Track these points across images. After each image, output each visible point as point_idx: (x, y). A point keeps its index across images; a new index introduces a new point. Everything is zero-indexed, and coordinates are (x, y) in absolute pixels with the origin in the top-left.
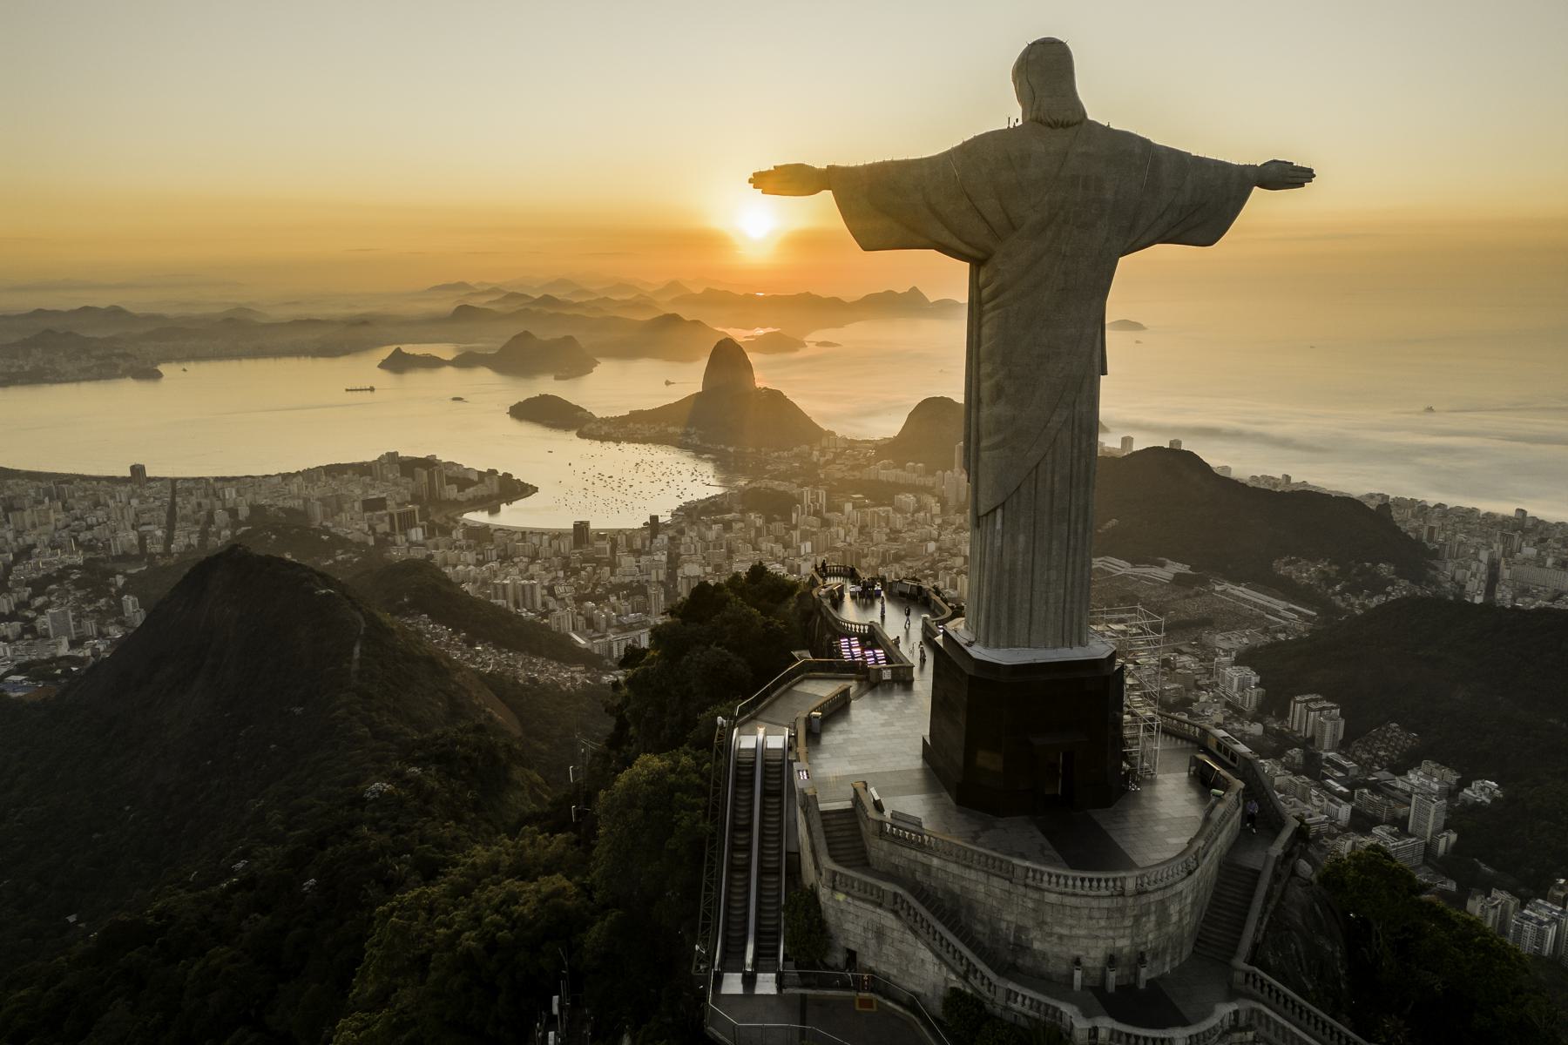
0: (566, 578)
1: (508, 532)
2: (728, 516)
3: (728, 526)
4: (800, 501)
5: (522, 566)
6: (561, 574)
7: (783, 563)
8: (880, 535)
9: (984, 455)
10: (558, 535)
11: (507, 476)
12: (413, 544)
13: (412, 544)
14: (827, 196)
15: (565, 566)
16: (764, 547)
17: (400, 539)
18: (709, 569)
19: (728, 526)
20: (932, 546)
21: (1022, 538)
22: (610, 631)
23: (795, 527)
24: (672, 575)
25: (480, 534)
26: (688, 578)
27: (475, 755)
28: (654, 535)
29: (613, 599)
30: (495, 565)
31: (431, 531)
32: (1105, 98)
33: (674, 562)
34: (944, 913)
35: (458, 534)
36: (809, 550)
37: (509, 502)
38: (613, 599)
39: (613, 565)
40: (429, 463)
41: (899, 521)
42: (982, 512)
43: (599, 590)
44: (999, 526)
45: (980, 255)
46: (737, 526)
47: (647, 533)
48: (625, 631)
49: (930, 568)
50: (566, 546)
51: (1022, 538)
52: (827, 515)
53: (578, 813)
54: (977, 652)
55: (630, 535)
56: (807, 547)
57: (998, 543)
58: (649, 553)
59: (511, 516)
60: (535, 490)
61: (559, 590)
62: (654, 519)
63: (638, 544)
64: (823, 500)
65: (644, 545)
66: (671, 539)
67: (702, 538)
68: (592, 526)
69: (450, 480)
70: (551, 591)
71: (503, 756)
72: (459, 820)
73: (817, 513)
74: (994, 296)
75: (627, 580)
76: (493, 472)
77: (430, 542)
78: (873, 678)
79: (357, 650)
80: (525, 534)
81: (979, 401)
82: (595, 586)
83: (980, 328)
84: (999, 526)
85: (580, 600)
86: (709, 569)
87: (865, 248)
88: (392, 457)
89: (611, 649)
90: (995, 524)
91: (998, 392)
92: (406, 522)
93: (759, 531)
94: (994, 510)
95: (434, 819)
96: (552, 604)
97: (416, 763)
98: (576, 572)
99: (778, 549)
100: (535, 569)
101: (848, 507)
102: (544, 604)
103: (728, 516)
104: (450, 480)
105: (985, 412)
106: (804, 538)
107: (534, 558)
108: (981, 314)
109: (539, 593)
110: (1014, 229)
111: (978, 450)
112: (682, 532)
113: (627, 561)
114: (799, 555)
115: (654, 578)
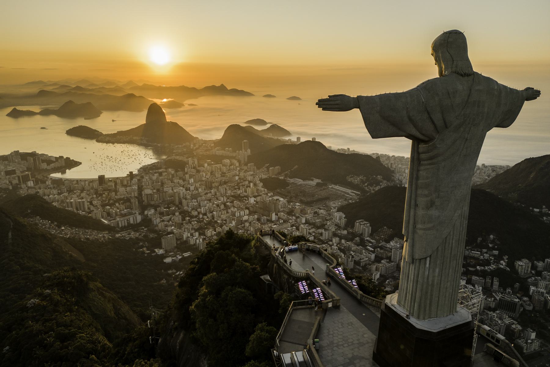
0: (97, 197)
1: (71, 181)
2: (160, 170)
3: (161, 174)
4: (188, 163)
5: (78, 194)
6: (95, 196)
7: (183, 187)
8: (218, 175)
9: (420, 232)
10: (92, 181)
11: (68, 159)
12: (29, 188)
13: (29, 187)
14: (356, 114)
15: (96, 193)
16: (175, 181)
17: (23, 186)
19: (161, 174)
20: (237, 178)
21: (437, 270)
23: (187, 173)
24: (140, 194)
25: (58, 183)
26: (147, 195)
27: (73, 280)
28: (131, 179)
29: (117, 204)
30: (66, 194)
31: (36, 182)
33: (140, 189)
35: (49, 183)
36: (193, 181)
37: (70, 169)
38: (117, 204)
39: (116, 191)
40: (33, 154)
41: (224, 169)
42: (417, 256)
43: (111, 201)
44: (428, 265)
45: (426, 139)
46: (164, 174)
47: (128, 178)
48: (123, 217)
49: (237, 186)
50: (95, 185)
51: (437, 270)
52: (199, 168)
53: (152, 340)
54: (413, 321)
55: (122, 179)
56: (192, 180)
57: (427, 273)
58: (130, 186)
59: (71, 174)
60: (81, 163)
61: (95, 202)
62: (131, 173)
63: (125, 183)
64: (196, 162)
65: (128, 183)
66: (139, 180)
67: (151, 179)
68: (106, 177)
69: (43, 161)
70: (91, 203)
71: (85, 279)
72: (71, 311)
73: (194, 168)
74: (431, 158)
75: (122, 197)
76: (61, 157)
77: (37, 187)
78: (324, 307)
80: (78, 181)
81: (416, 205)
82: (109, 200)
83: (418, 171)
84: (428, 265)
85: (103, 206)
86: (155, 191)
87: (373, 138)
88: (17, 153)
89: (118, 224)
90: (425, 264)
91: (431, 204)
92: (25, 179)
94: (426, 258)
95: (61, 313)
96: (92, 208)
97: (48, 287)
98: (101, 195)
99: (181, 182)
100: (83, 195)
101: (206, 165)
102: (89, 208)
103: (160, 170)
104: (43, 161)
105: (421, 212)
106: (191, 177)
107: (83, 190)
108: (419, 164)
109: (86, 204)
110: (446, 127)
111: (415, 227)
112: (142, 177)
113: (122, 190)
114: (189, 184)
115: (133, 195)
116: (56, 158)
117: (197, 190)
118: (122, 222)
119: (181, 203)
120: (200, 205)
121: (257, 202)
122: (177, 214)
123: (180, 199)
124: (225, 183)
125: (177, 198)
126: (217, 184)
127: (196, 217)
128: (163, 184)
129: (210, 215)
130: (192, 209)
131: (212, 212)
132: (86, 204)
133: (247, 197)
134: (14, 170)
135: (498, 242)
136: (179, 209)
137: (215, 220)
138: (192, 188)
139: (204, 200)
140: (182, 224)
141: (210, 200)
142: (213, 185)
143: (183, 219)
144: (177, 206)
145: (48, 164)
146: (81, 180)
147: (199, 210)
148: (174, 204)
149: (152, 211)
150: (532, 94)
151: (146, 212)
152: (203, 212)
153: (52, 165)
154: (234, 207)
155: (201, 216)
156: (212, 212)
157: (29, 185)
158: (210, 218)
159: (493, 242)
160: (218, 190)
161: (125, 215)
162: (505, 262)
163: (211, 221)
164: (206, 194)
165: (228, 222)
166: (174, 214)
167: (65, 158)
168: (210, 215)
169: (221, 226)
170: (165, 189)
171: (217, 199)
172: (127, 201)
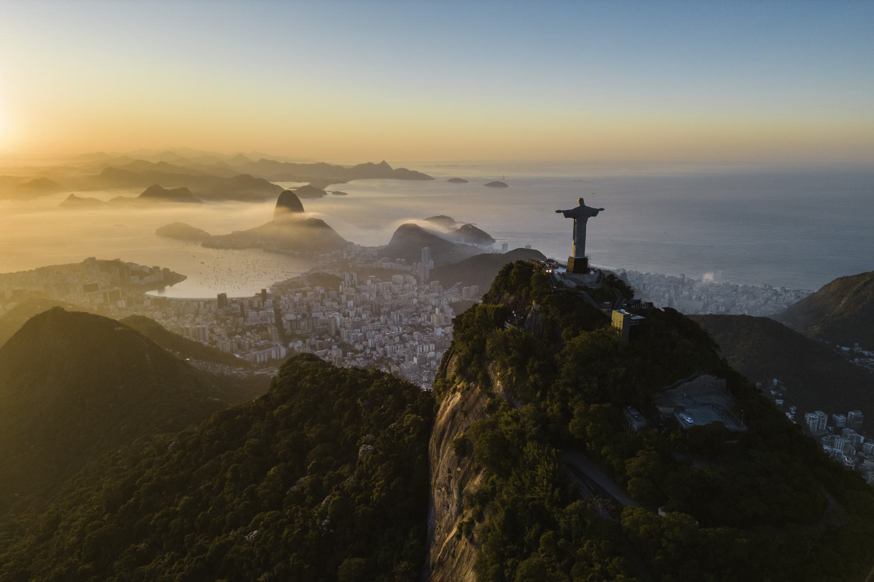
1: (179, 301)
3: (305, 294)
4: (343, 280)
6: (215, 322)
7: (339, 311)
8: (388, 297)
10: (208, 302)
13: (118, 310)
15: (217, 317)
16: (327, 304)
18: (299, 316)
20: (415, 301)
22: (252, 350)
23: (342, 293)
25: (163, 303)
26: (291, 321)
29: (248, 334)
30: (175, 319)
32: (587, 204)
33: (279, 314)
34: (575, 280)
35: (147, 303)
37: (171, 285)
39: (244, 315)
40: (117, 263)
41: (397, 289)
43: (240, 330)
46: (309, 294)
47: (260, 299)
48: (260, 349)
49: (416, 312)
50: (214, 308)
52: (359, 287)
55: (251, 301)
58: (263, 309)
59: (171, 292)
61: (218, 330)
62: (264, 291)
63: (256, 305)
64: (355, 278)
65: (259, 305)
66: (274, 302)
68: (228, 296)
69: (134, 273)
73: (353, 286)
75: (254, 324)
76: (157, 268)
79: (147, 356)
80: (189, 302)
82: (236, 328)
85: (231, 335)
86: (299, 316)
88: (92, 260)
89: (255, 358)
93: (323, 295)
99: (335, 304)
100: (198, 320)
101: (369, 282)
102: (210, 338)
103: (303, 289)
104: (134, 273)
106: (349, 298)
107: (197, 314)
113: (252, 314)
116: (150, 269)
117: (360, 316)
118: (261, 357)
119: (338, 333)
120: (365, 337)
121: (446, 335)
122: (335, 347)
123: (336, 327)
124: (399, 308)
125: (333, 326)
126: (387, 310)
127: (361, 352)
128: (309, 309)
129: (380, 350)
130: (355, 342)
131: (383, 346)
132: (207, 332)
133: (432, 327)
134: (96, 285)
135: (784, 389)
136: (336, 341)
137: (389, 356)
138: (352, 313)
139: (371, 331)
140: (344, 361)
141: (379, 330)
142: (382, 310)
143: (345, 355)
144: (334, 337)
145: (141, 278)
146: (193, 300)
147: (364, 343)
148: (330, 335)
149: (300, 343)
150: (602, 209)
151: (291, 345)
152: (370, 345)
153: (147, 279)
154: (414, 340)
155: (368, 351)
156: (383, 346)
157: (120, 306)
158: (381, 354)
159: (777, 388)
160: (389, 317)
161: (262, 348)
162: (791, 414)
163: (382, 358)
164: (373, 322)
165: (406, 359)
166: (330, 348)
167: (162, 269)
168: (380, 350)
169: (398, 364)
170: (314, 315)
171: (389, 329)
172: (261, 329)
